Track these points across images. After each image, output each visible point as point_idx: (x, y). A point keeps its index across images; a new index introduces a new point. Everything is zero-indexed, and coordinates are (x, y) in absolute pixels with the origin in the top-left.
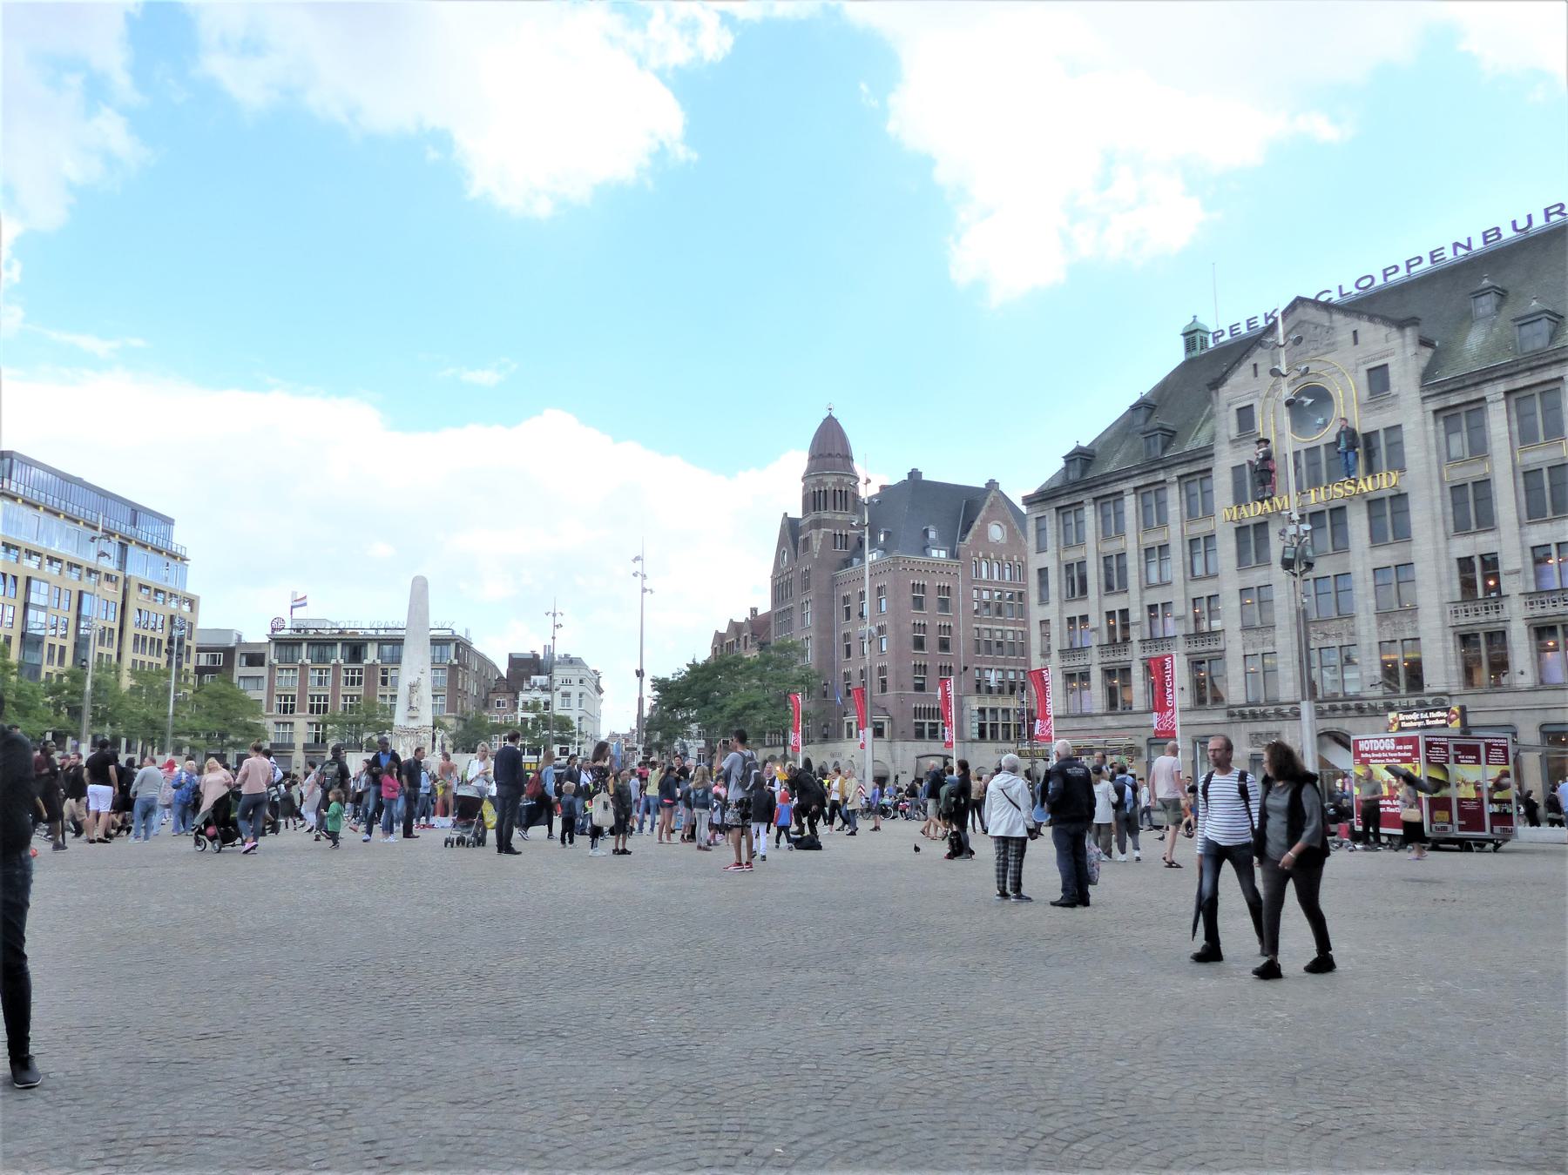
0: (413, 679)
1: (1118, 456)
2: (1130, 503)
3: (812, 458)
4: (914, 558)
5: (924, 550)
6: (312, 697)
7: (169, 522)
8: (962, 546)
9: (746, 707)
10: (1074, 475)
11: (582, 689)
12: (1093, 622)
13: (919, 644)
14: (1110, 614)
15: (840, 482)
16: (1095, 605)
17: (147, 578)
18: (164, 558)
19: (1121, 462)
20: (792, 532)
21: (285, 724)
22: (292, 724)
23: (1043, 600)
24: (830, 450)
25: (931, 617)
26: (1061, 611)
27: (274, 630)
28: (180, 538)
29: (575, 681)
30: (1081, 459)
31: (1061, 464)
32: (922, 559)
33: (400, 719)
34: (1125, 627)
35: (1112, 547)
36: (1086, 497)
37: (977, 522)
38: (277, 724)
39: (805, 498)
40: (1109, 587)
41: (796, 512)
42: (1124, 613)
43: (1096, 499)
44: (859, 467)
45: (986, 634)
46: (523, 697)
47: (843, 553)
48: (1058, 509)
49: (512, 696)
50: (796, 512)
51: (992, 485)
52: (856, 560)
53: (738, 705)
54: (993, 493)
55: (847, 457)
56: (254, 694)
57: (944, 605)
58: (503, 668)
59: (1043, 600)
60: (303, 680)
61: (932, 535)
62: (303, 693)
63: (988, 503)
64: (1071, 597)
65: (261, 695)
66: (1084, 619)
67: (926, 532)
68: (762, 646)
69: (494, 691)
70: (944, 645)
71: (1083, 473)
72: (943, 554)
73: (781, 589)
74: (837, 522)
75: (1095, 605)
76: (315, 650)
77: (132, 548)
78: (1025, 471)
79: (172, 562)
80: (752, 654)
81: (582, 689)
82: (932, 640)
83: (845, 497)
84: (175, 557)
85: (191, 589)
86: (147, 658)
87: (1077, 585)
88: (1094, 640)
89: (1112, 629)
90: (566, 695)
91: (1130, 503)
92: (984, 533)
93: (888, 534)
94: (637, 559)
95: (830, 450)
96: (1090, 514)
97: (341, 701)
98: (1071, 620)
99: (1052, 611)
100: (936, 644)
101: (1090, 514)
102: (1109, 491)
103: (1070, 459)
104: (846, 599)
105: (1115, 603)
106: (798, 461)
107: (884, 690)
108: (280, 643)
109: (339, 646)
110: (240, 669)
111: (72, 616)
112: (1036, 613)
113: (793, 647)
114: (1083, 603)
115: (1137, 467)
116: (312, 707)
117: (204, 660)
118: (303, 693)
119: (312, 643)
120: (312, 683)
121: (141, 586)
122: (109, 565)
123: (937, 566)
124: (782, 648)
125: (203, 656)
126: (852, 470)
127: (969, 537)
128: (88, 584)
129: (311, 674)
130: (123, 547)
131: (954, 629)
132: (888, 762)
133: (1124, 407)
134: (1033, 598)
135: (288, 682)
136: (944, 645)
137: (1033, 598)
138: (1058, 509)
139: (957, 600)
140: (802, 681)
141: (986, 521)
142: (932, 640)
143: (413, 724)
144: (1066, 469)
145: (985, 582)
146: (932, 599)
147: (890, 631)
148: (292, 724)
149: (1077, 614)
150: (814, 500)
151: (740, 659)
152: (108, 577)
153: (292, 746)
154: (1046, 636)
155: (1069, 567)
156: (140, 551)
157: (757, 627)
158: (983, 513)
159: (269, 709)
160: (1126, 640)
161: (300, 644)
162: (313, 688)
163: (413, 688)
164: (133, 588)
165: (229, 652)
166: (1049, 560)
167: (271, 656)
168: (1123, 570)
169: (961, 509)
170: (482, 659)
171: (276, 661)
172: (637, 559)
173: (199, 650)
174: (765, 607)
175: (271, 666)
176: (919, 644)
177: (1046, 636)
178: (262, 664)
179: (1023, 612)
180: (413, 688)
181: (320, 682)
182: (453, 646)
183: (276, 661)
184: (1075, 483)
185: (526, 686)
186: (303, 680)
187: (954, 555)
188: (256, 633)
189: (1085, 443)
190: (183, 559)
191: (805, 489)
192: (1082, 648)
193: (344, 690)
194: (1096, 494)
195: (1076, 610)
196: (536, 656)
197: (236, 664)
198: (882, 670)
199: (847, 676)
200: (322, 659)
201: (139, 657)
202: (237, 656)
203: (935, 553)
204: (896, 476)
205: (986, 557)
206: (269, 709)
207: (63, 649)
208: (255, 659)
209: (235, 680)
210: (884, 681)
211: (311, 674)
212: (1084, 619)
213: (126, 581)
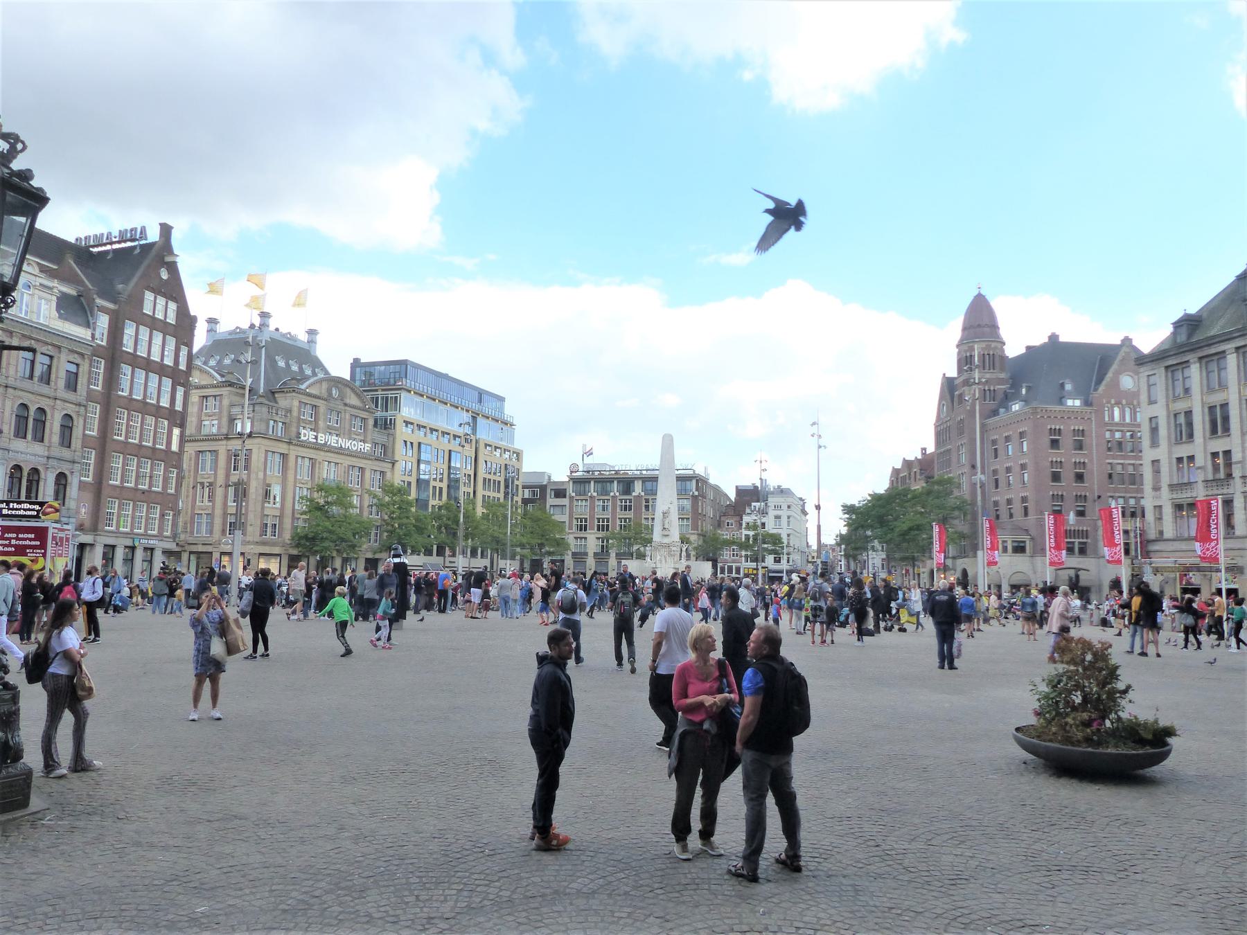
0: (665, 509)
1: (1222, 322)
2: (1232, 360)
3: (964, 329)
4: (1050, 407)
5: (1061, 400)
7: (502, 399)
8: (1095, 395)
9: (911, 529)
10: (1182, 338)
11: (789, 513)
12: (1199, 461)
13: (1056, 477)
14: (1215, 455)
15: (988, 347)
16: (1201, 447)
17: (490, 440)
18: (500, 425)
19: (1223, 328)
20: (949, 386)
23: (1154, 443)
24: (980, 322)
25: (1067, 455)
26: (1170, 453)
28: (509, 411)
29: (785, 507)
30: (1189, 324)
31: (1170, 329)
32: (1058, 408)
33: (657, 536)
34: (1229, 464)
35: (1217, 399)
36: (1191, 357)
37: (1110, 375)
39: (959, 361)
40: (1214, 431)
41: (953, 373)
42: (1227, 453)
43: (1201, 358)
44: (1004, 333)
45: (1119, 468)
46: (746, 519)
47: (992, 404)
48: (1167, 368)
49: (737, 518)
50: (953, 373)
51: (1127, 341)
52: (1002, 410)
53: (905, 527)
54: (1124, 349)
55: (994, 327)
56: (558, 517)
57: (1079, 446)
58: (732, 495)
59: (1154, 443)
60: (592, 508)
61: (1068, 387)
62: (592, 517)
63: (1119, 357)
64: (1179, 441)
65: (565, 518)
66: (1191, 458)
67: (1062, 385)
68: (929, 478)
70: (1080, 477)
71: (1190, 336)
72: (1078, 403)
73: (943, 433)
74: (992, 381)
75: (1201, 447)
77: (480, 420)
78: (1151, 335)
79: (505, 428)
80: (918, 486)
81: (789, 513)
82: (1068, 475)
83: (994, 359)
85: (517, 445)
86: (492, 494)
87: (1185, 432)
88: (1199, 477)
89: (1216, 468)
90: (778, 517)
91: (1232, 360)
92: (1116, 383)
93: (1029, 389)
94: (814, 424)
95: (980, 322)
96: (1195, 371)
97: (618, 523)
98: (1180, 460)
99: (1162, 453)
100: (1072, 476)
101: (1195, 371)
102: (1213, 351)
103: (1178, 325)
104: (994, 442)
105: (1219, 445)
106: (954, 331)
107: (1026, 514)
108: (577, 481)
110: (551, 501)
111: (445, 467)
112: (1148, 455)
113: (950, 481)
114: (1227, 439)
115: (1238, 330)
117: (527, 494)
118: (592, 517)
119: (597, 481)
120: (598, 510)
121: (486, 445)
123: (1073, 412)
124: (940, 483)
125: (526, 491)
126: (998, 336)
127: (1102, 388)
129: (597, 503)
130: (474, 418)
131: (1089, 466)
132: (1030, 573)
133: (1230, 278)
134: (1146, 442)
135: (582, 509)
136: (1080, 477)
137: (1146, 442)
138: (1167, 368)
139: (1092, 440)
140: (959, 508)
141: (1118, 373)
142: (1068, 475)
143: (666, 540)
144: (1174, 334)
145: (1117, 424)
146: (1067, 441)
147: (1030, 467)
149: (1185, 455)
150: (965, 362)
151: (907, 491)
153: (586, 554)
154: (1157, 472)
155: (1212, 409)
156: (485, 421)
157: (925, 465)
158: (1114, 367)
159: (571, 528)
160: (1229, 476)
162: (599, 514)
163: (665, 514)
164: (482, 446)
165: (543, 488)
166: (1160, 411)
167: (570, 491)
168: (1226, 419)
169: (1092, 365)
170: (716, 489)
172: (814, 424)
173: (524, 487)
174: (931, 449)
175: (571, 498)
176: (1056, 477)
177: (1157, 472)
179: (1137, 450)
180: (665, 514)
182: (694, 482)
184: (1182, 346)
185: (748, 511)
186: (592, 508)
187: (1087, 403)
188: (560, 475)
189: (1193, 309)
191: (959, 353)
192: (1190, 484)
193: (621, 514)
194: (1201, 354)
195: (1184, 451)
196: (756, 487)
198: (1024, 499)
199: (996, 503)
200: (605, 492)
201: (487, 493)
203: (1070, 402)
204: (1039, 339)
205: (1117, 403)
206: (571, 528)
207: (441, 489)
208: (560, 493)
210: (1026, 508)
211: (597, 503)
212: (1191, 458)
213: (477, 442)
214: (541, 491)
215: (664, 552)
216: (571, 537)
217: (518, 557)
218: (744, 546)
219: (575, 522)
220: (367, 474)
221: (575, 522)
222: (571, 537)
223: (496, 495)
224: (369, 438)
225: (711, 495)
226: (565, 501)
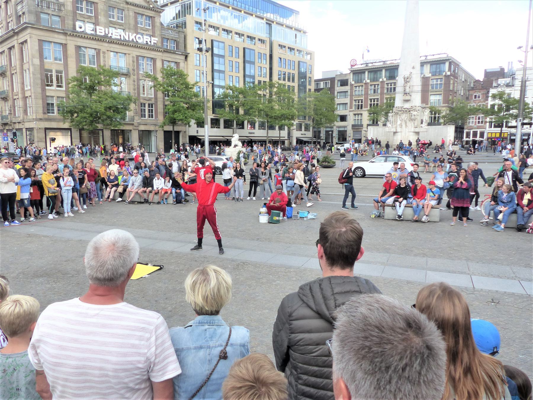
0: (407, 74)
6: (371, 100)
21: (358, 114)
22: (361, 114)
27: (352, 66)
33: (398, 103)
38: (355, 115)
46: (493, 91)
49: (484, 91)
65: (347, 100)
69: (473, 89)
76: (372, 75)
77: (274, 25)
84: (300, 31)
85: (310, 49)
108: (358, 73)
109: (384, 71)
110: (338, 88)
111: (241, 61)
116: (371, 105)
118: (366, 99)
120: (371, 92)
122: (264, 35)
125: (322, 83)
128: (248, 44)
130: (270, 25)
143: (407, 106)
148: (361, 114)
152: (262, 41)
156: (279, 27)
159: (351, 108)
161: (364, 73)
165: (332, 80)
167: (351, 81)
171: (353, 83)
175: (352, 85)
178: (347, 85)
180: (407, 80)
181: (375, 92)
182: (447, 64)
183: (353, 83)
185: (494, 84)
188: (345, 69)
190: (304, 32)
197: (336, 86)
202: (336, 81)
206: (351, 108)
208: (344, 83)
209: (336, 93)
211: (370, 87)
214: (331, 83)
215: (404, 116)
216: (352, 114)
217: (286, 128)
218: (491, 111)
219: (354, 103)
220: (159, 64)
221: (354, 103)
222: (352, 114)
223: (291, 84)
224: (158, 33)
225: (463, 77)
226: (347, 88)
